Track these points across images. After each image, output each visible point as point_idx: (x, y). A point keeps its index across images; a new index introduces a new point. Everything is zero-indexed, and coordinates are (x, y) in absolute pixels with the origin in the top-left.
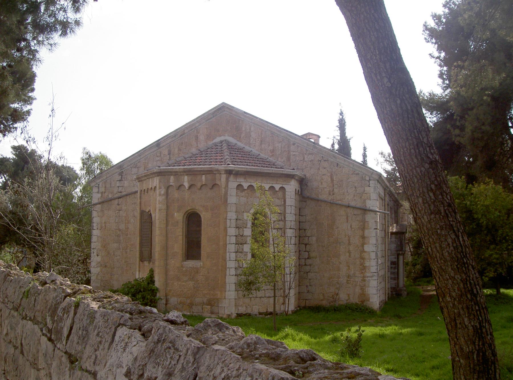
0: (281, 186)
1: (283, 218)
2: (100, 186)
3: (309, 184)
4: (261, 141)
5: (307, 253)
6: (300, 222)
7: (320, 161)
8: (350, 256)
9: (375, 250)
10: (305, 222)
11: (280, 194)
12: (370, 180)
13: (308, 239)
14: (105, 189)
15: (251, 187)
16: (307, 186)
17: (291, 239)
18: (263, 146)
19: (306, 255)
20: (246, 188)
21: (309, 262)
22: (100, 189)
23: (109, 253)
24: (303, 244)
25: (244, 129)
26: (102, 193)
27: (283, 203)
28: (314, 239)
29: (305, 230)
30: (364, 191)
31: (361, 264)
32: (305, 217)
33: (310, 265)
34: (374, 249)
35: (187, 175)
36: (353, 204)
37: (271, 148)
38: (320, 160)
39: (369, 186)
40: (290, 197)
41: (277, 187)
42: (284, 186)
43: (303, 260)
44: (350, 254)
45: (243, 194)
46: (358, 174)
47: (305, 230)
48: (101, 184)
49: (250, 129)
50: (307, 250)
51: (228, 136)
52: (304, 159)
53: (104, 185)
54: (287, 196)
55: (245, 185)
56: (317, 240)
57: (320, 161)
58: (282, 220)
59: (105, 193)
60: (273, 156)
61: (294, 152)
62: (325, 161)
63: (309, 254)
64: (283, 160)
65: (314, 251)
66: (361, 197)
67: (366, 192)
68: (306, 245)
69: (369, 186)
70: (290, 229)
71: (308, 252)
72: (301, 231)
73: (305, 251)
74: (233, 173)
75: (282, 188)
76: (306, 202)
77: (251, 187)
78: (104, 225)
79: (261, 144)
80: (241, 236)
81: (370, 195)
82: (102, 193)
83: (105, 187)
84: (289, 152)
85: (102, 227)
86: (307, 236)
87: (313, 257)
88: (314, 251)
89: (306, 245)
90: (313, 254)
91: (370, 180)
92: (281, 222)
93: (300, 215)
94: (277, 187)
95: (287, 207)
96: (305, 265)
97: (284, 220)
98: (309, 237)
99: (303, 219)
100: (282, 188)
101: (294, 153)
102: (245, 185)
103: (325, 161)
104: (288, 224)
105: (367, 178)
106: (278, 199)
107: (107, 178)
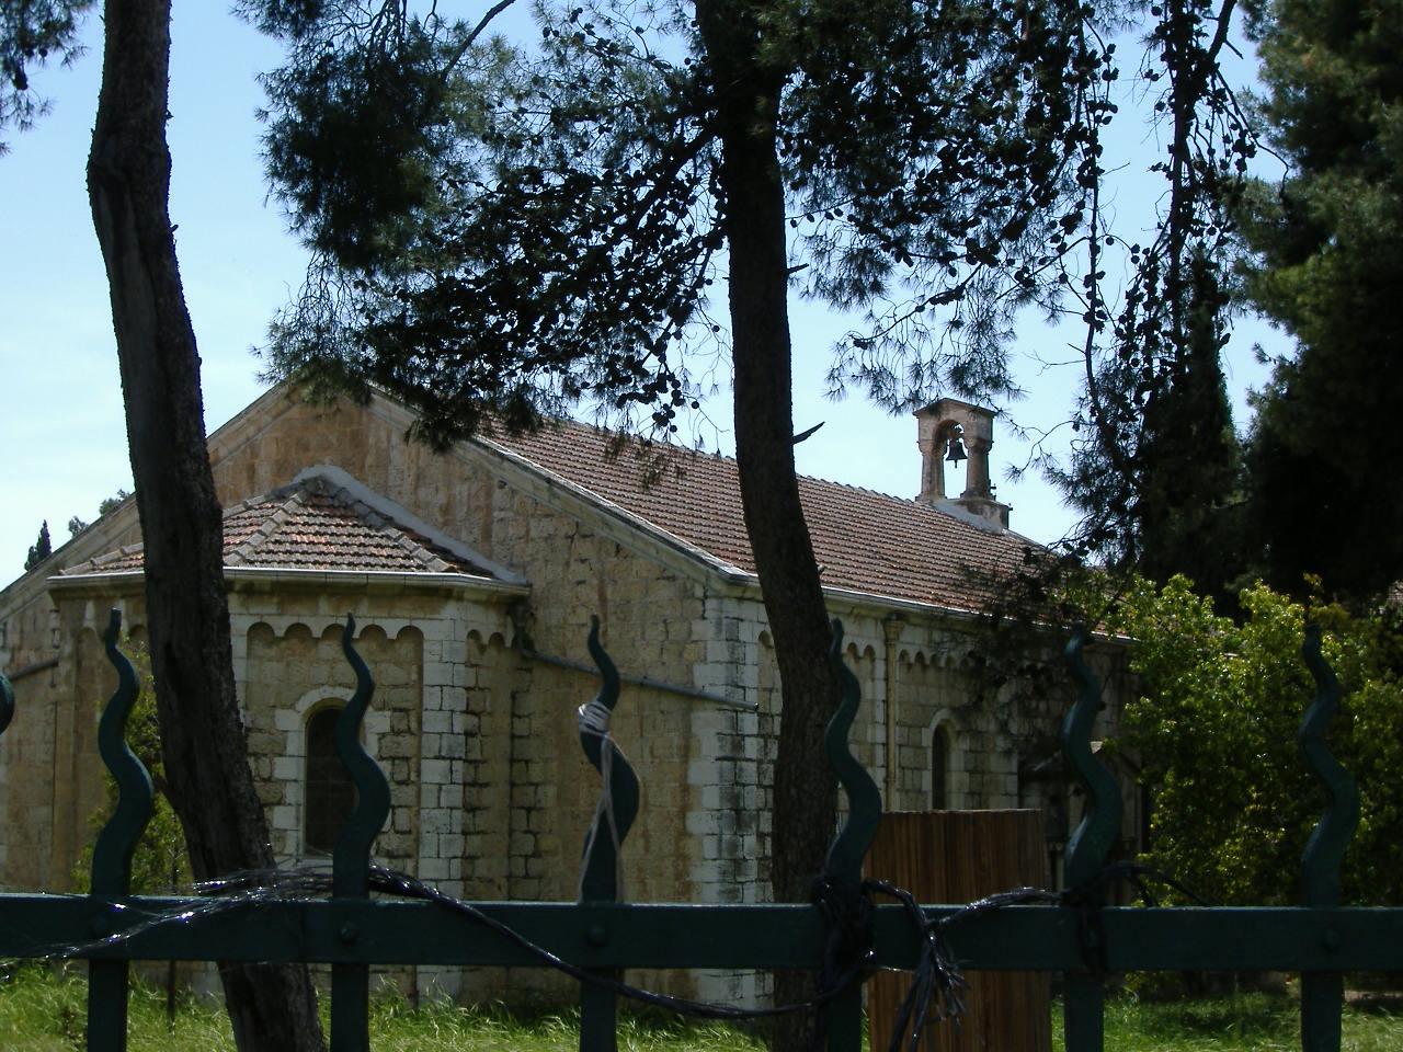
0: (406, 623)
1: (414, 725)
2: (9, 627)
3: (540, 614)
4: (418, 478)
5: (531, 838)
6: (513, 737)
7: (572, 537)
8: (647, 849)
9: (717, 831)
10: (528, 737)
11: (406, 649)
12: (706, 597)
13: (536, 793)
14: (22, 638)
15: (298, 631)
16: (535, 620)
17: (440, 790)
18: (423, 493)
19: (528, 844)
20: (280, 633)
21: (536, 866)
22: (9, 636)
23: (27, 837)
24: (522, 808)
25: (371, 441)
26: (13, 650)
27: (414, 677)
28: (551, 791)
29: (527, 762)
30: (690, 632)
31: (678, 877)
32: (527, 720)
33: (540, 877)
34: (713, 826)
35: (123, 597)
36: (657, 675)
37: (441, 499)
38: (570, 533)
39: (704, 618)
40: (437, 658)
41: (392, 628)
42: (416, 624)
43: (521, 861)
44: (647, 842)
45: (273, 652)
46: (673, 578)
47: (527, 762)
48: (10, 621)
49: (389, 440)
50: (531, 828)
51: (333, 463)
52: (528, 531)
53: (18, 626)
54: (426, 656)
55: (280, 625)
56: (559, 797)
57: (572, 537)
58: (409, 731)
59: (20, 648)
60: (446, 523)
61: (502, 510)
62: (585, 536)
63: (536, 842)
64: (472, 539)
65: (551, 831)
66: (680, 655)
67: (694, 637)
68: (529, 810)
69: (704, 618)
70: (436, 758)
71: (535, 834)
72: (516, 766)
73: (526, 832)
74: (237, 587)
75: (411, 633)
76: (529, 670)
77: (298, 631)
78: (15, 750)
79: (417, 487)
80: (265, 780)
81: (705, 648)
82: (13, 650)
83: (22, 632)
84: (489, 509)
85: (11, 756)
86: (532, 784)
87: (547, 852)
88: (551, 831)
89: (529, 810)
90: (547, 843)
91: (706, 597)
92: (408, 736)
93: (513, 715)
94: (392, 628)
95: (425, 689)
96: (527, 876)
97: (419, 732)
98: (537, 785)
99: (521, 727)
100: (411, 633)
101: (502, 514)
102: (280, 625)
103: (585, 536)
104: (431, 744)
105: (699, 592)
106: (396, 664)
107: (25, 603)
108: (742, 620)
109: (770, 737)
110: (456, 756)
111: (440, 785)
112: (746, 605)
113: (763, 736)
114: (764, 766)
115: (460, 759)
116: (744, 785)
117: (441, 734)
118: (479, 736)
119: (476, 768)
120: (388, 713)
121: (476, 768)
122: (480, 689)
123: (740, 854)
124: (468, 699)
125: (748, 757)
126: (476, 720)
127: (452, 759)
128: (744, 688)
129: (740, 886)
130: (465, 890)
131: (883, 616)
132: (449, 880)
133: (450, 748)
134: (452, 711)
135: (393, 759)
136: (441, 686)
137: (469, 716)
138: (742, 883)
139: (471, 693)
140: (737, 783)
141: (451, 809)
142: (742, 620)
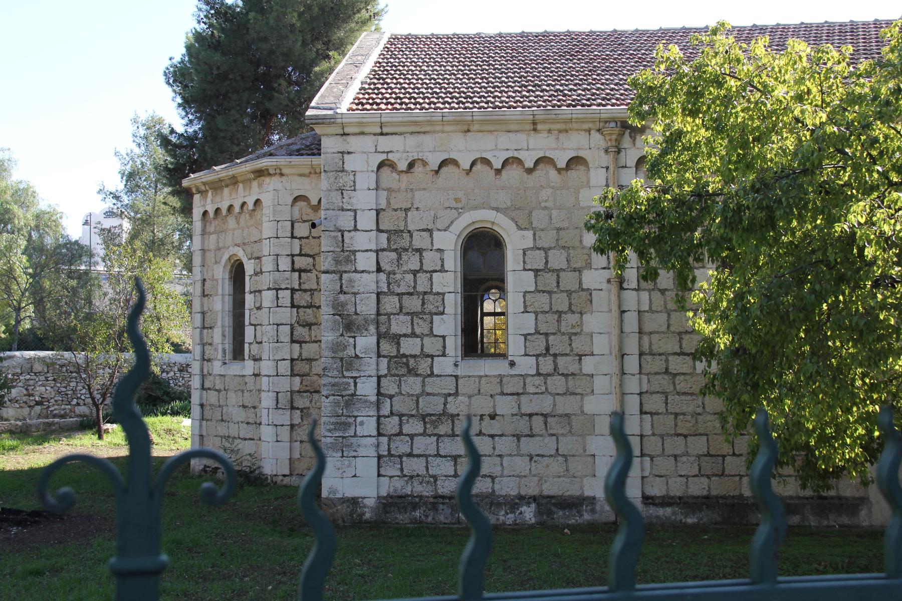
70: (269, 289)
108: (349, 153)
109: (407, 250)
110: (283, 286)
111: (270, 308)
112: (350, 139)
113: (395, 250)
114: (398, 276)
115: (287, 289)
116: (355, 294)
117: (269, 272)
118: (314, 271)
119: (312, 295)
120: (253, 261)
121: (312, 295)
122: (314, 238)
123: (350, 352)
124: (301, 245)
125: (360, 268)
126: (311, 260)
127: (277, 290)
128: (355, 211)
129: (351, 381)
130: (301, 383)
131: (597, 126)
132: (277, 375)
133: (275, 282)
134: (277, 255)
135: (255, 292)
136: (269, 238)
137: (303, 258)
138: (355, 378)
139: (304, 241)
140: (342, 291)
141: (278, 325)
142: (349, 153)
